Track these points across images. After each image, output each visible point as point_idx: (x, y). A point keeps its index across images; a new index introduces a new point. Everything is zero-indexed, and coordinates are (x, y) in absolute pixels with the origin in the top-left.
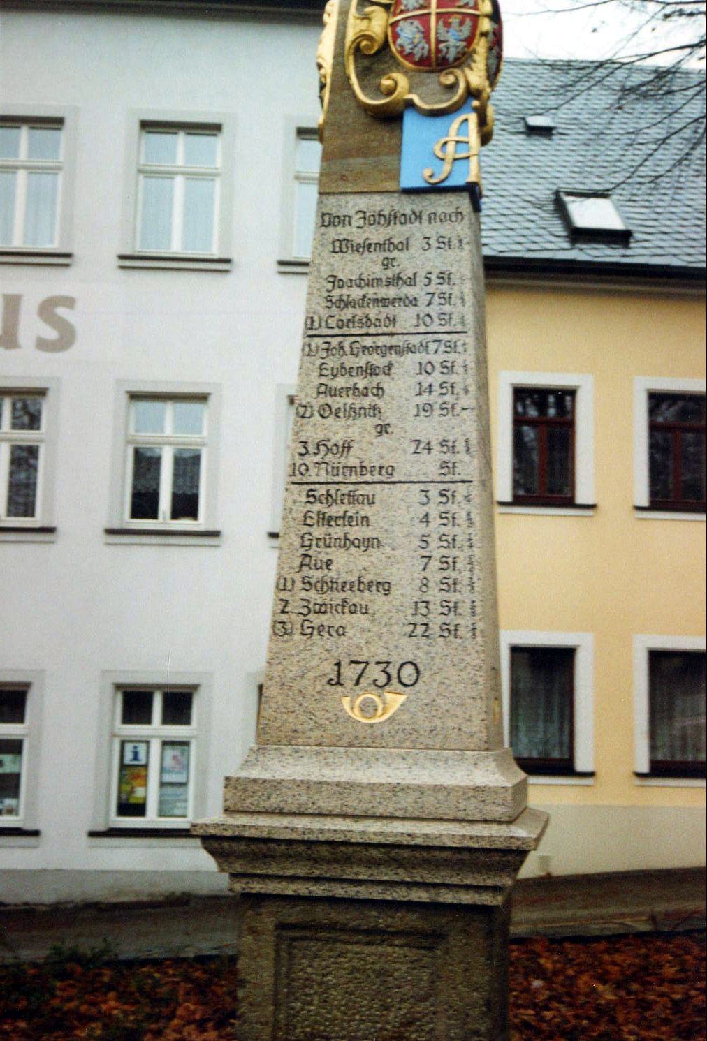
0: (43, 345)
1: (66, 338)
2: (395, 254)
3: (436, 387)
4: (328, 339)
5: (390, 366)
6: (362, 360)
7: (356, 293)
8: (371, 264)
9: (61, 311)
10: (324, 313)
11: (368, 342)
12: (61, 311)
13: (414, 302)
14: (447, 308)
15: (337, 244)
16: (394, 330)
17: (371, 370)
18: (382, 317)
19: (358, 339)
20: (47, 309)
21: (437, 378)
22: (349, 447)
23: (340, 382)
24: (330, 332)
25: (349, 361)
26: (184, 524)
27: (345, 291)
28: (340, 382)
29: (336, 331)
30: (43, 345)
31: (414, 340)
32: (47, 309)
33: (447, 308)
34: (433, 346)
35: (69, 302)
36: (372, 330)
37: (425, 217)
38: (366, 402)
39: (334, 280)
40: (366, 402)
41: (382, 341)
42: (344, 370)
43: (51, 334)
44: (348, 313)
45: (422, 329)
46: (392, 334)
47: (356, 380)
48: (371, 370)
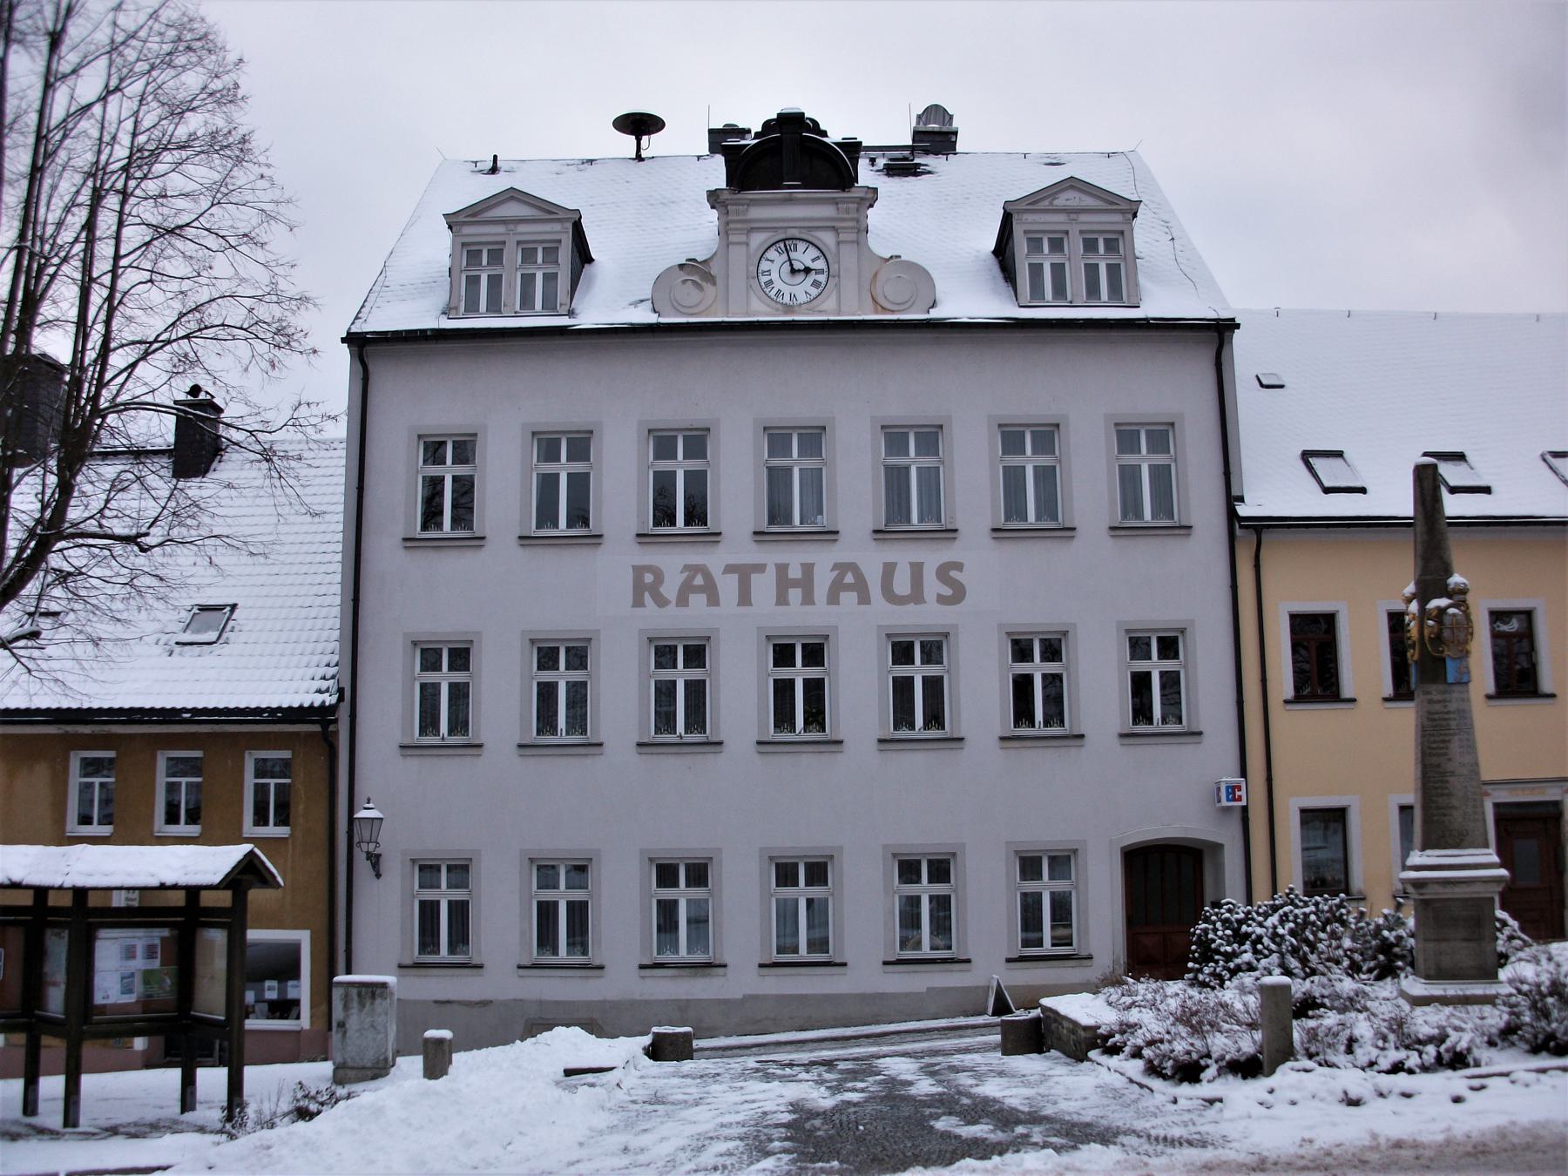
0: (942, 599)
1: (958, 594)
6: (1442, 738)
8: (1437, 707)
9: (954, 574)
12: (954, 574)
13: (1455, 719)
17: (1444, 742)
20: (943, 572)
23: (1434, 745)
25: (1437, 739)
26: (1055, 730)
28: (1434, 745)
30: (942, 599)
32: (943, 572)
35: (959, 566)
42: (1435, 742)
43: (947, 591)
44: (1435, 723)
48: (1444, 742)
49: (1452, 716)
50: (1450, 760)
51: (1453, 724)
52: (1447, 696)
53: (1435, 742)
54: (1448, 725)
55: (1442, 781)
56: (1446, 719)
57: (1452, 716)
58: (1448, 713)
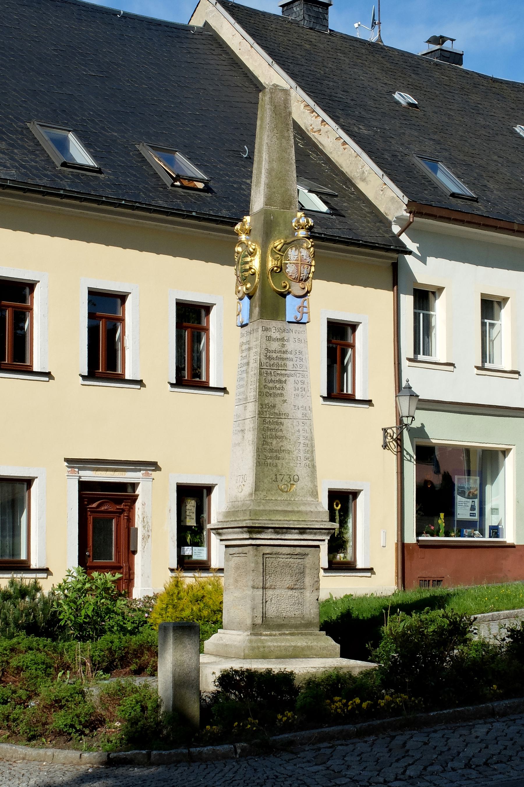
2: (285, 343)
3: (300, 389)
4: (267, 370)
5: (286, 381)
7: (274, 355)
10: (265, 361)
11: (279, 372)
14: (301, 363)
15: (267, 337)
16: (286, 369)
17: (280, 381)
18: (283, 364)
19: (276, 370)
21: (300, 386)
22: (275, 406)
23: (271, 385)
24: (267, 368)
27: (271, 354)
28: (271, 385)
29: (269, 368)
31: (293, 372)
33: (301, 363)
34: (298, 375)
36: (280, 368)
37: (294, 331)
38: (279, 392)
39: (267, 350)
40: (279, 392)
41: (283, 372)
42: (271, 381)
44: (272, 362)
45: (295, 369)
46: (286, 370)
47: (276, 384)
48: (280, 381)
49: (289, 356)
50: (284, 401)
51: (290, 364)
52: (285, 335)
53: (271, 381)
54: (285, 365)
55: (277, 423)
56: (283, 359)
57: (289, 356)
58: (284, 352)
